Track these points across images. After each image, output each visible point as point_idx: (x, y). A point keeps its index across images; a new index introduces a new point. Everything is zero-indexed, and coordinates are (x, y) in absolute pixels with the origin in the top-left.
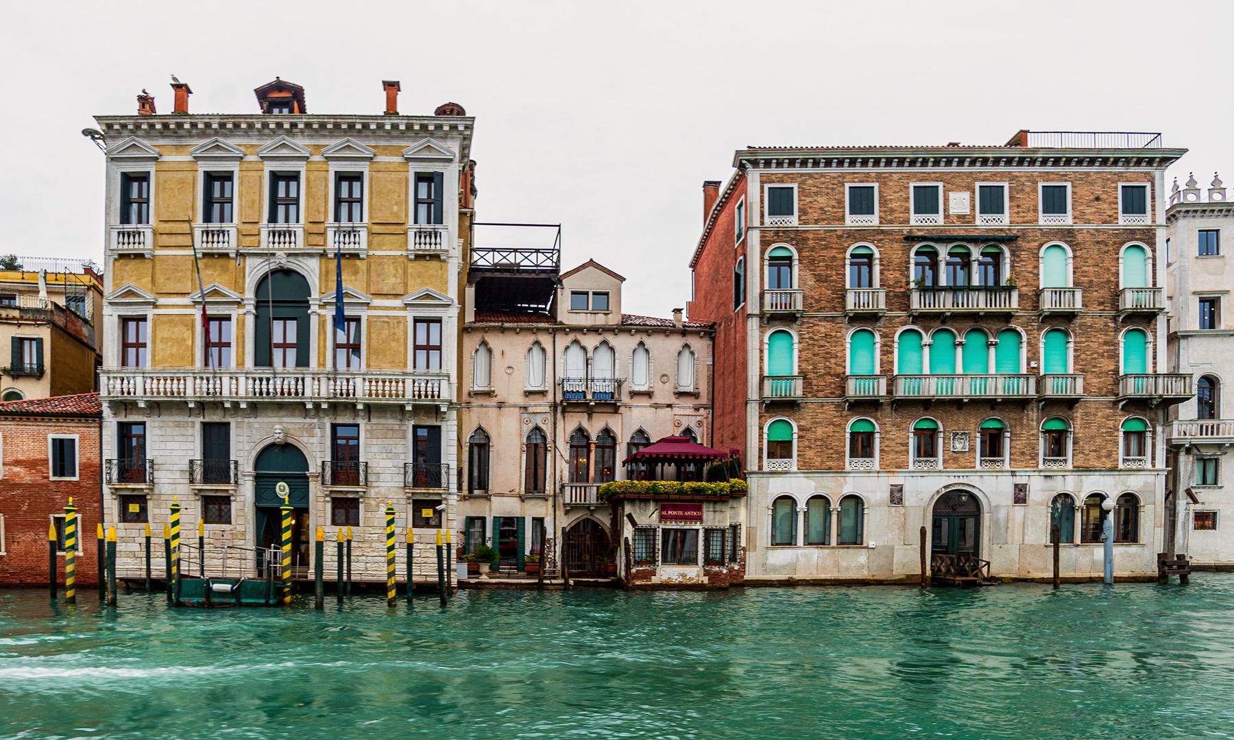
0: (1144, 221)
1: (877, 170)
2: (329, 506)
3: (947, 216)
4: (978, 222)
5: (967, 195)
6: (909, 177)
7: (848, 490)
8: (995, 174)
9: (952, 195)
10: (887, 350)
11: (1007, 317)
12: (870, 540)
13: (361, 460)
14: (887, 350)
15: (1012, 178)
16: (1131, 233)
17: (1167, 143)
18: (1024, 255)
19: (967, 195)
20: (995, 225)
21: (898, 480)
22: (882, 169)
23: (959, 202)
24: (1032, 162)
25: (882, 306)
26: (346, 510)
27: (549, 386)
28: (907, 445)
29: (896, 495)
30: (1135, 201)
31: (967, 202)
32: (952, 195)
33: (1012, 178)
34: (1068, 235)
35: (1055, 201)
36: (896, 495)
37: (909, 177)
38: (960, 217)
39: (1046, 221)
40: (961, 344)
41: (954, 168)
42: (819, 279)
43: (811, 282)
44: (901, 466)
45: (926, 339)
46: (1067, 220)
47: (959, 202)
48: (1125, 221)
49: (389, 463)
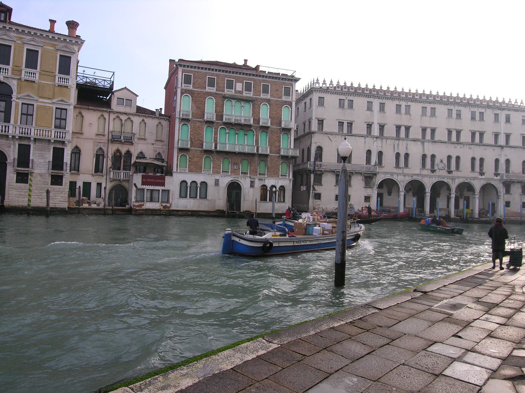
0: (289, 99)
1: (216, 73)
2: (15, 175)
3: (235, 91)
4: (244, 94)
5: (241, 84)
6: (226, 76)
7: (203, 180)
8: (250, 78)
9: (237, 84)
10: (216, 134)
11: (250, 126)
12: (209, 197)
13: (31, 158)
14: (216, 134)
15: (254, 80)
16: (286, 103)
17: (297, 76)
18: (256, 106)
19: (241, 84)
20: (248, 95)
21: (217, 178)
22: (217, 73)
23: (239, 87)
24: (260, 76)
25: (215, 119)
26: (22, 178)
27: (106, 132)
28: (220, 166)
29: (217, 183)
30: (288, 92)
31: (241, 87)
32: (237, 84)
33: (254, 80)
34: (268, 101)
35: (266, 91)
36: (217, 183)
37: (226, 76)
38: (239, 92)
39: (263, 96)
40: (237, 133)
41: (238, 75)
42: (198, 108)
43: (195, 108)
44: (218, 173)
45: (227, 131)
46: (268, 96)
47: (239, 87)
48: (284, 98)
49: (42, 161)
